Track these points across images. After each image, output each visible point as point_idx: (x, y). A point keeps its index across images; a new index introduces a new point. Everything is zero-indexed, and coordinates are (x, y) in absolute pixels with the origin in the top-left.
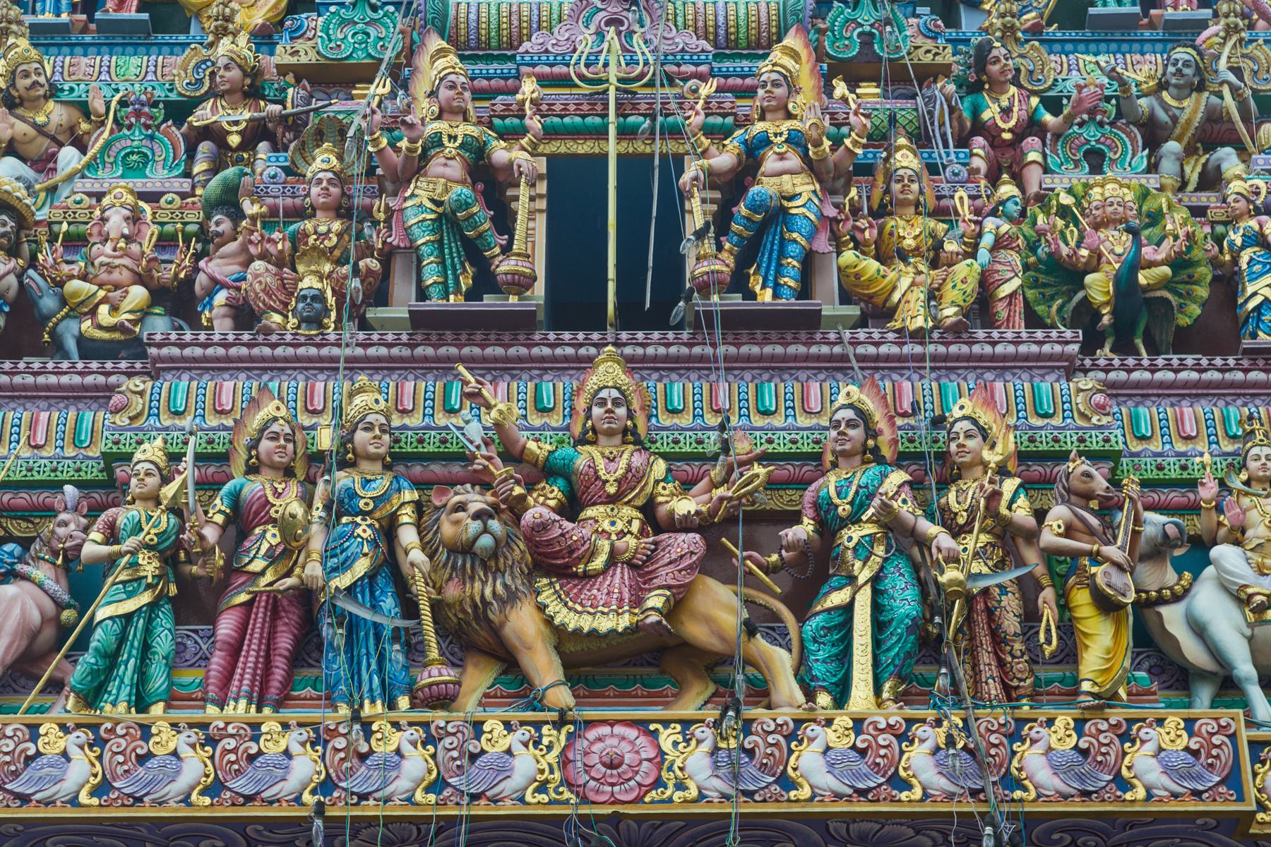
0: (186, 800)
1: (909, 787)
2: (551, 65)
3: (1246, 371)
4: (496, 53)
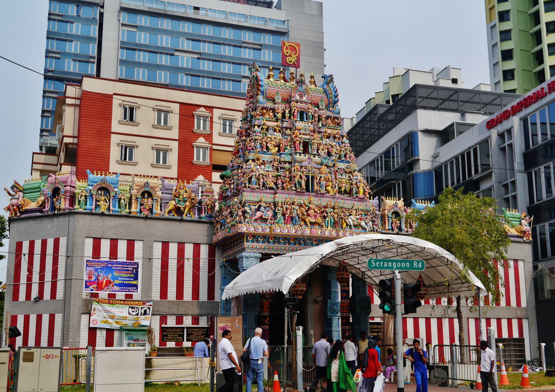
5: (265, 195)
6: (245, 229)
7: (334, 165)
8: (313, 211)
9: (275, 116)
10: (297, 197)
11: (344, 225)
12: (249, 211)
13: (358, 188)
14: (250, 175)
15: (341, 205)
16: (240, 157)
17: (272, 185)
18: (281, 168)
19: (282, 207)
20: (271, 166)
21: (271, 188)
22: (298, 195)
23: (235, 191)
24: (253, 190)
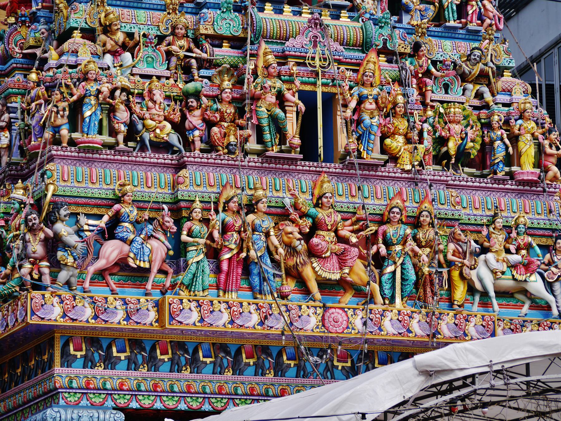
0: (224, 325)
1: (412, 332)
2: (295, 52)
3: (492, 184)
4: (275, 41)
5: (139, 173)
6: (57, 311)
7: (417, 47)
8: (330, 236)
10: (267, 179)
11: (460, 292)
12: (73, 239)
13: (514, 139)
14: (78, 93)
15: (446, 210)
16: (34, 18)
17: (167, 133)
18: (202, 64)
19: (206, 221)
20: (161, 57)
21: (163, 147)
22: (270, 170)
23: (16, 158)
24: (88, 154)
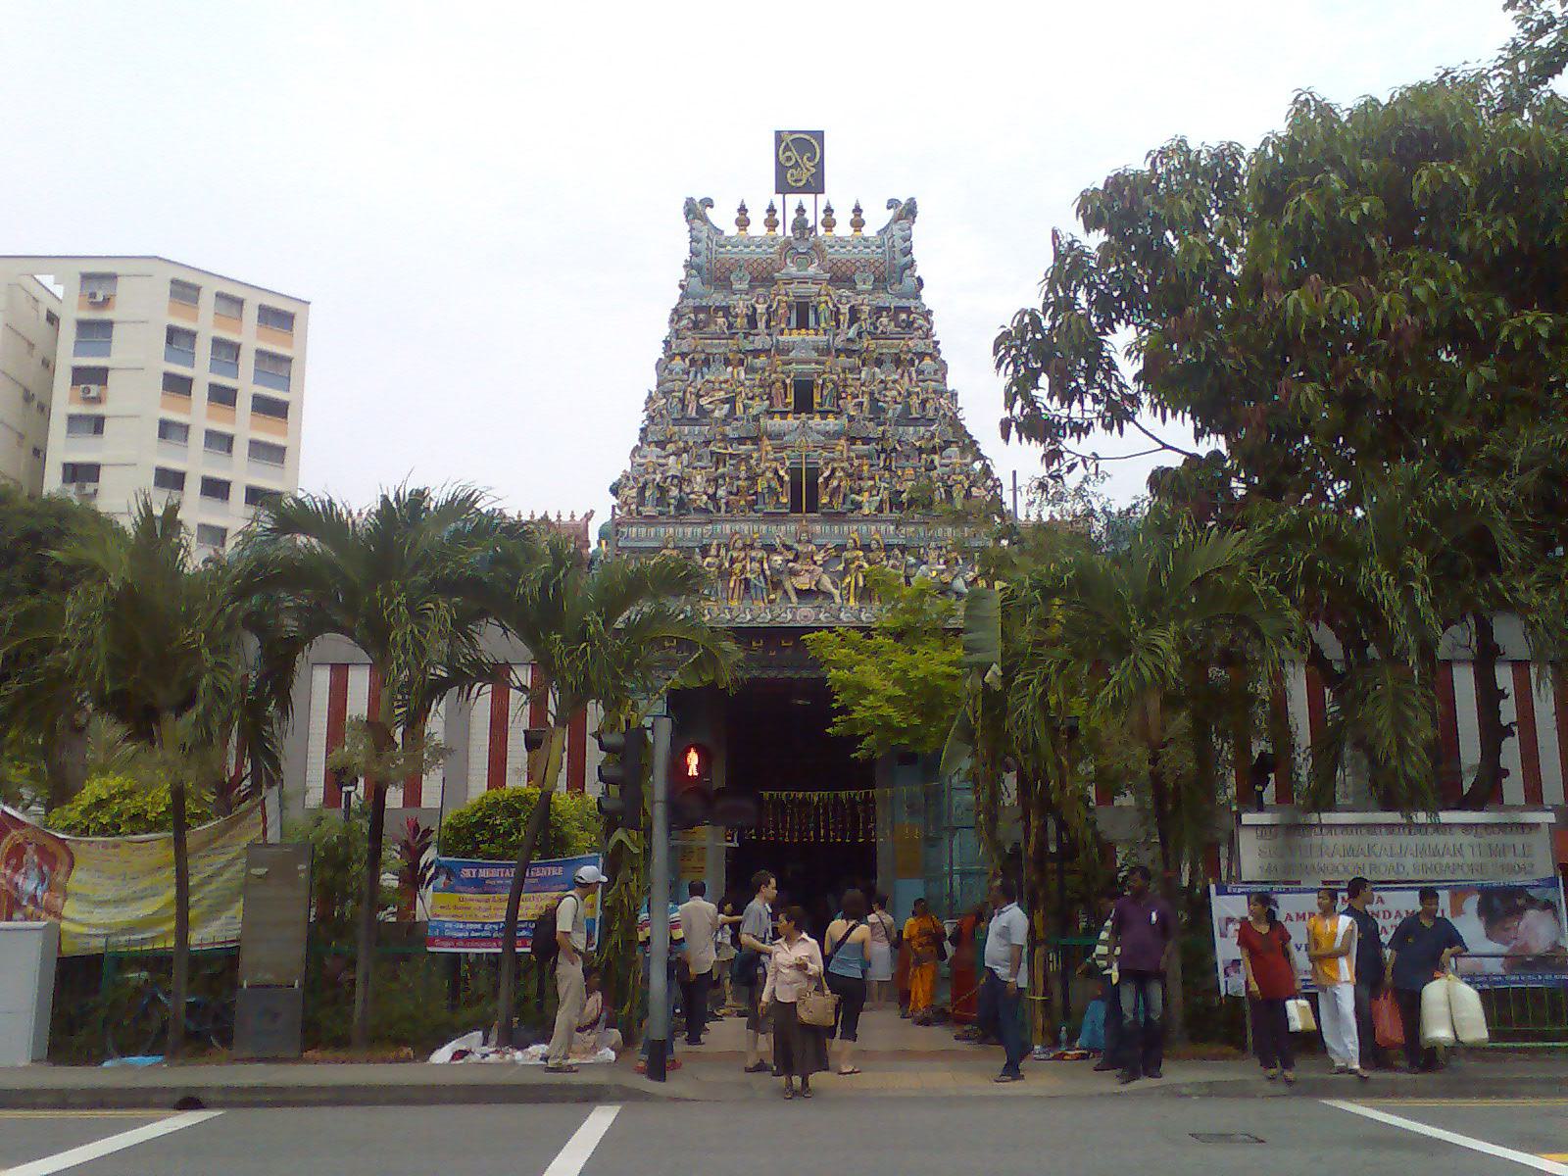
9: (730, 326)
